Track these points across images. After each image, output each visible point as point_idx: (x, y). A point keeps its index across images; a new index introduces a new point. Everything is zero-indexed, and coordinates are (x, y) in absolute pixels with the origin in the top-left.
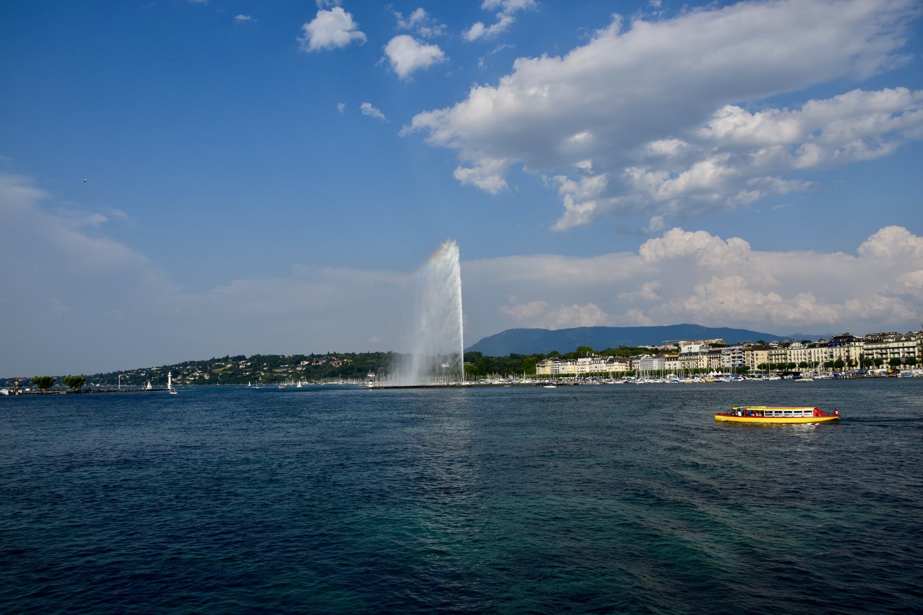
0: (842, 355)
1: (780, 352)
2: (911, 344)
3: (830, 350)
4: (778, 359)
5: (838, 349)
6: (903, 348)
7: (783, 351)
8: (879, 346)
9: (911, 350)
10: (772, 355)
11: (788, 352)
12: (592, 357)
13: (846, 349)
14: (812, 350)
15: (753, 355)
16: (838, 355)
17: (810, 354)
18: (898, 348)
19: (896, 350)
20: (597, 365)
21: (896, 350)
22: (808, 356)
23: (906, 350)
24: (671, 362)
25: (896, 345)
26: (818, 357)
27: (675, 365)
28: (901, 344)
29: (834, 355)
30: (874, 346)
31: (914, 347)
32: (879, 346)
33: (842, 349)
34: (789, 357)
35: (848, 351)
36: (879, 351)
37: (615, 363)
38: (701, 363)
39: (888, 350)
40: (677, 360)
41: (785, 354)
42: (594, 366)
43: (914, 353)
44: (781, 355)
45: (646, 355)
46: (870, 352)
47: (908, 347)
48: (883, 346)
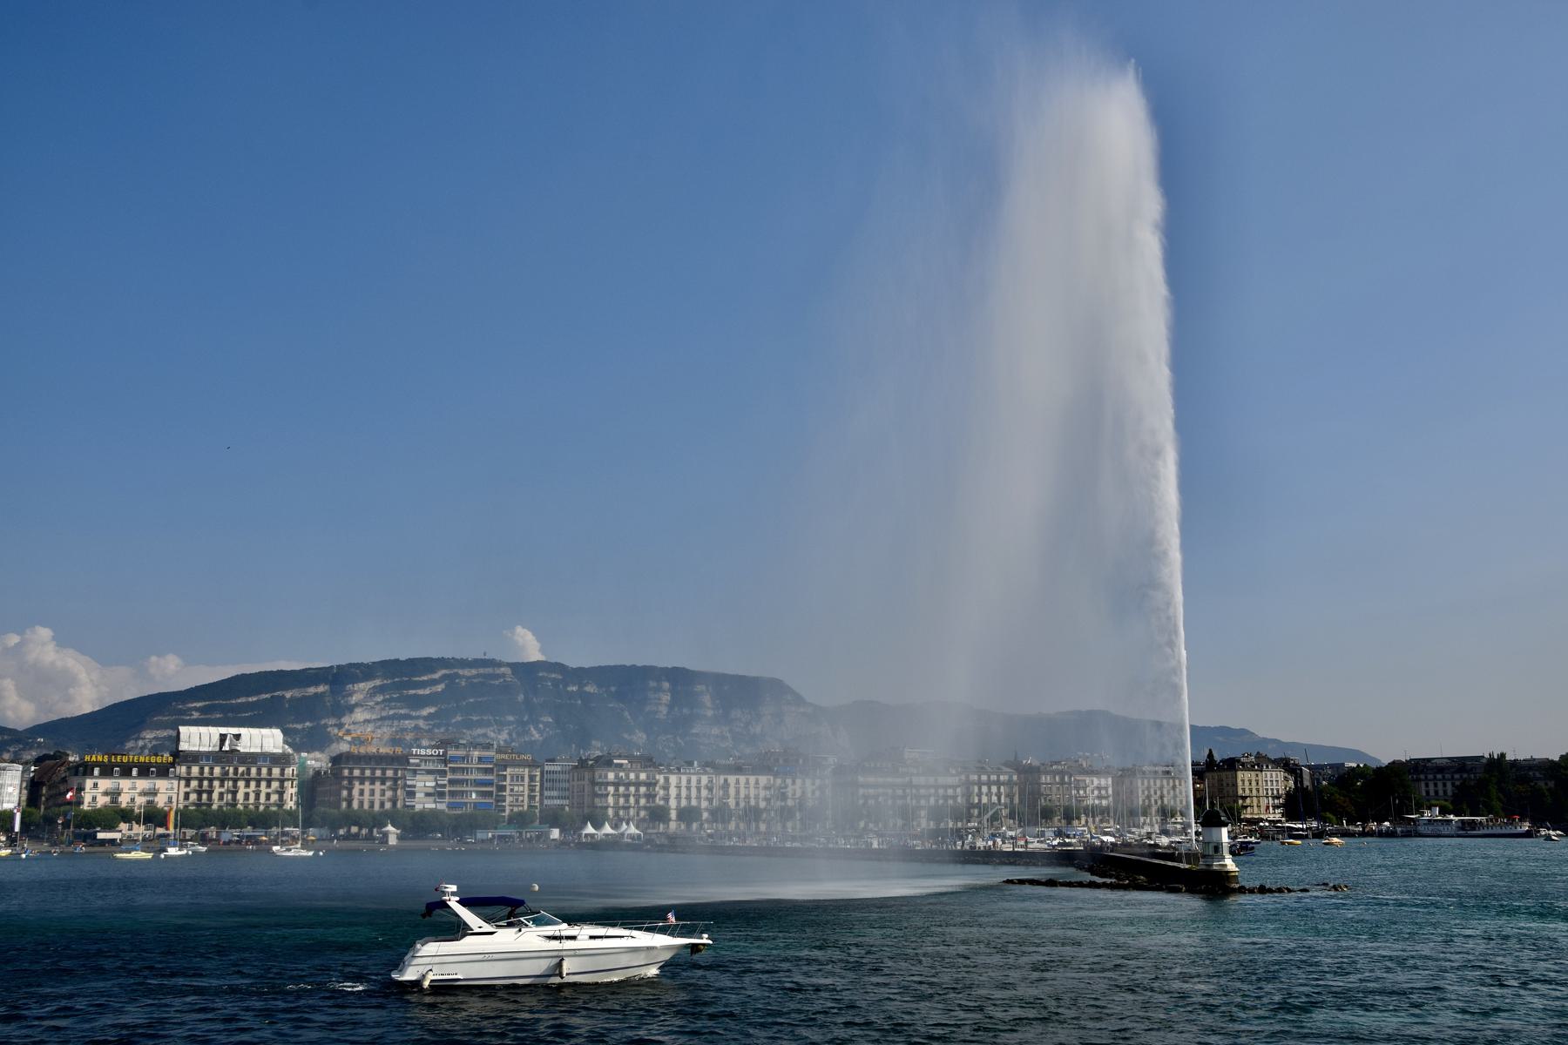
3: (779, 781)
4: (627, 797)
6: (937, 787)
7: (643, 776)
8: (890, 780)
9: (950, 792)
10: (608, 784)
11: (661, 778)
13: (818, 782)
14: (732, 779)
16: (798, 794)
18: (927, 787)
19: (922, 791)
21: (922, 791)
22: (718, 793)
24: (125, 784)
25: (921, 780)
26: (747, 797)
27: (154, 792)
28: (931, 780)
29: (790, 795)
30: (881, 780)
31: (954, 787)
32: (890, 780)
33: (808, 782)
36: (890, 791)
39: (908, 791)
41: (651, 784)
43: (954, 797)
44: (638, 784)
46: (871, 791)
47: (946, 787)
48: (899, 780)
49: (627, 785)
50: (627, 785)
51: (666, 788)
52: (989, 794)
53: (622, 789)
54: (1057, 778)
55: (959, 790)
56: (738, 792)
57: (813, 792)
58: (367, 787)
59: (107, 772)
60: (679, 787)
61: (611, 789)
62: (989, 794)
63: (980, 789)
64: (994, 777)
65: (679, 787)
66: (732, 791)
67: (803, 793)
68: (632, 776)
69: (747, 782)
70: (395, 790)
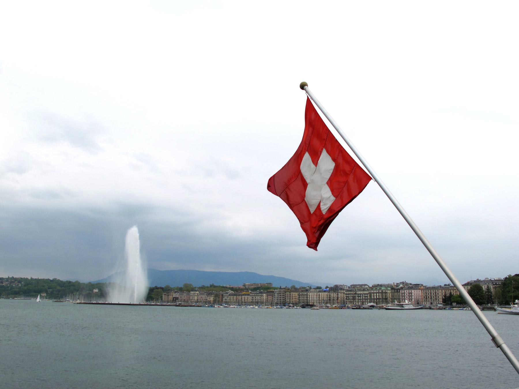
0: (335, 296)
1: (304, 293)
2: (366, 292)
3: (329, 294)
4: (303, 297)
5: (333, 294)
9: (366, 295)
11: (309, 294)
12: (199, 291)
14: (320, 294)
15: (290, 294)
16: (333, 296)
17: (319, 295)
20: (202, 296)
23: (364, 295)
24: (246, 297)
31: (367, 294)
34: (308, 296)
35: (338, 295)
37: (213, 296)
38: (263, 298)
40: (249, 295)
41: (307, 295)
42: (200, 296)
43: (367, 297)
44: (305, 295)
45: (231, 292)
47: (365, 294)
49: (303, 295)
50: (303, 295)
51: (310, 296)
52: (376, 296)
53: (302, 296)
54: (396, 291)
55: (368, 295)
56: (322, 296)
57: (336, 296)
58: (269, 297)
59: (244, 295)
60: (311, 296)
61: (301, 296)
62: (376, 296)
63: (374, 294)
64: (378, 291)
65: (311, 296)
66: (321, 296)
67: (334, 296)
68: (304, 293)
69: (323, 294)
70: (272, 297)
